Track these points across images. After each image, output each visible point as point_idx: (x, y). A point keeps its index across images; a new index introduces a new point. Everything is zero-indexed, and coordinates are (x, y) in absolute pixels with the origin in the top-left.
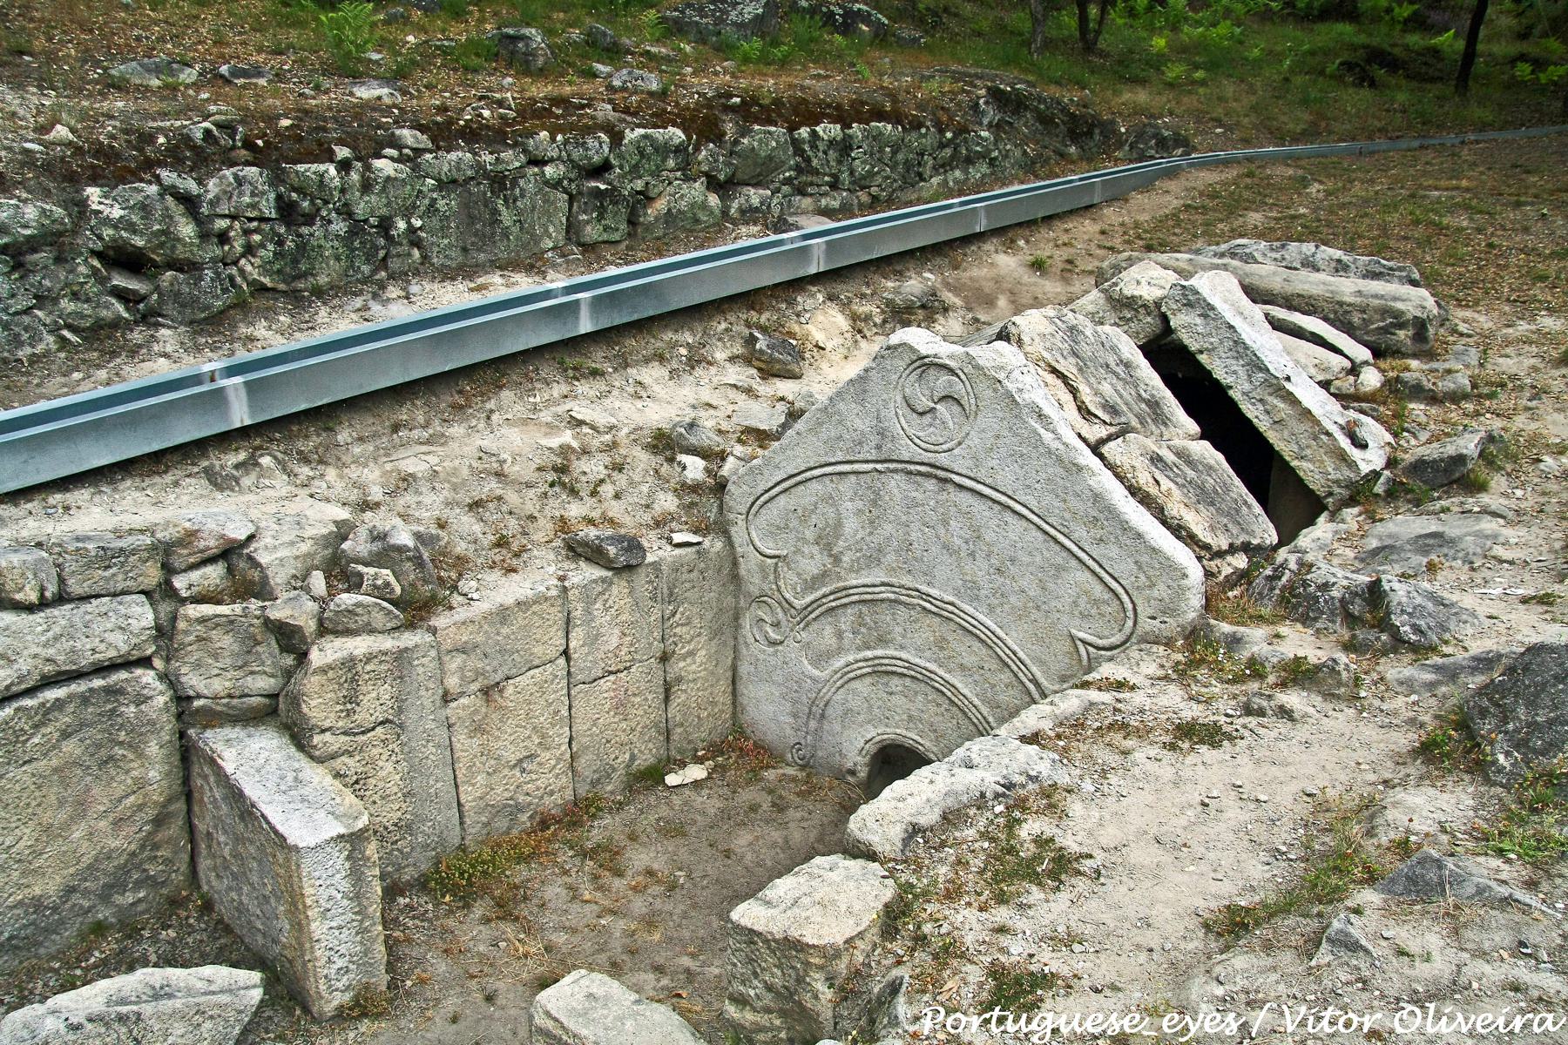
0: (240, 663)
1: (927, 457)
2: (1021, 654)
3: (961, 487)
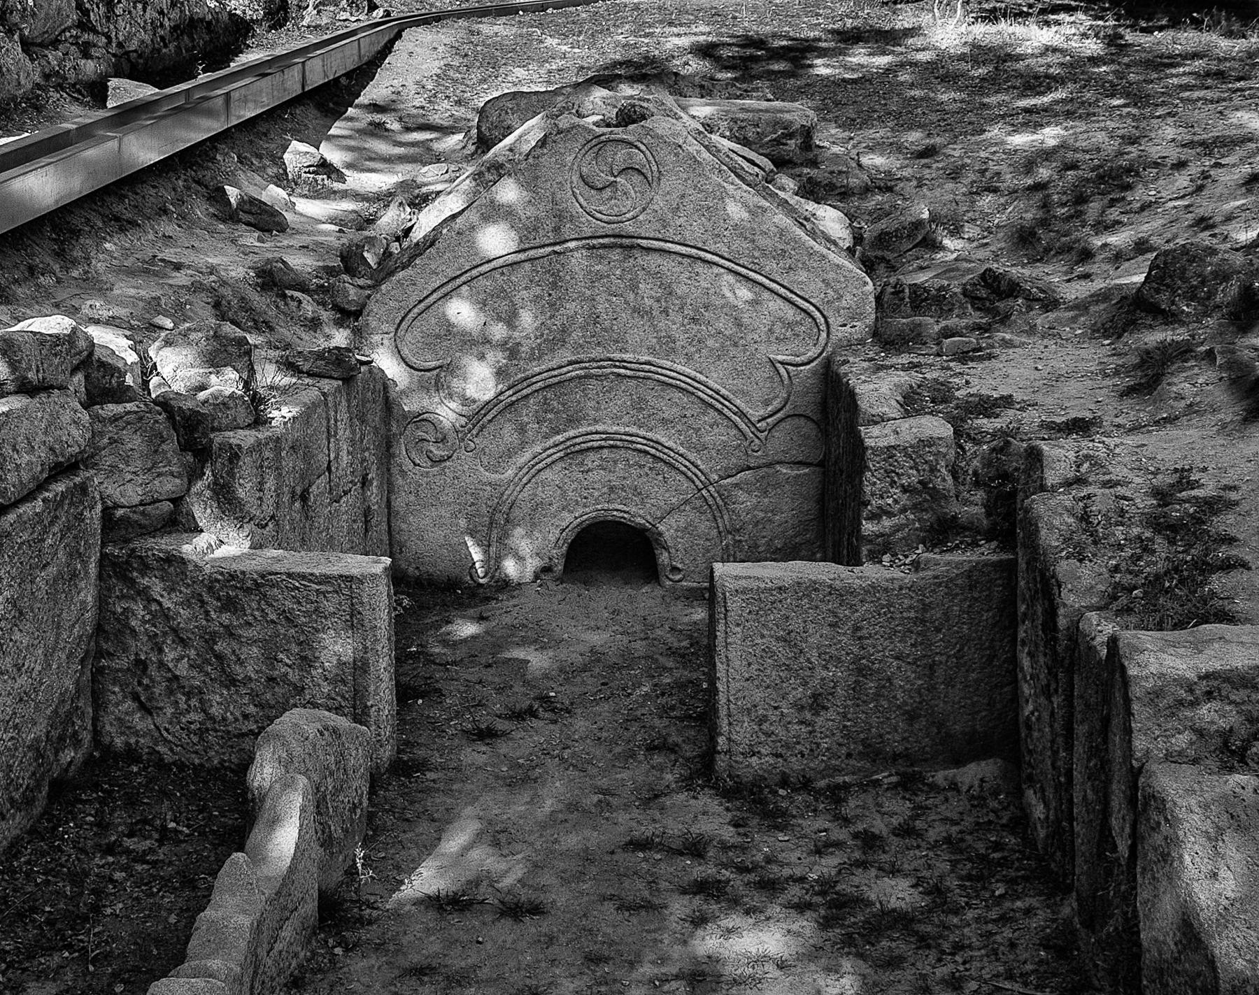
0: (149, 465)
2: (723, 391)
3: (648, 249)
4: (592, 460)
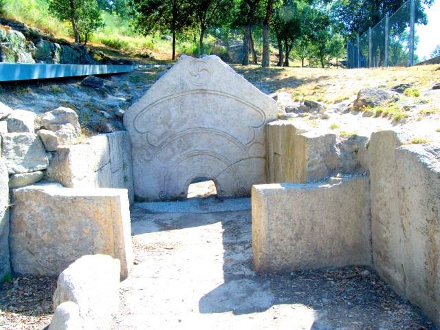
1: (198, 88)
4: (195, 158)
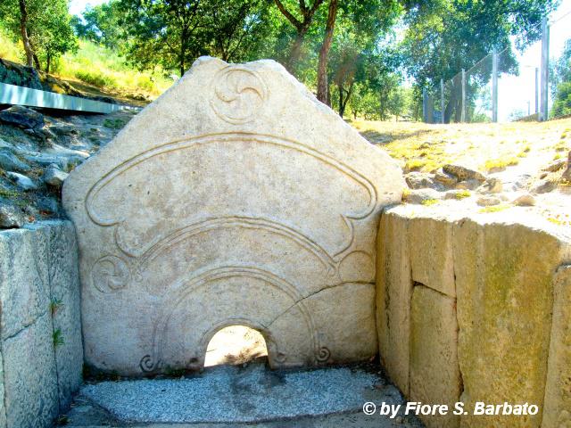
1: (236, 129)
4: (223, 285)
